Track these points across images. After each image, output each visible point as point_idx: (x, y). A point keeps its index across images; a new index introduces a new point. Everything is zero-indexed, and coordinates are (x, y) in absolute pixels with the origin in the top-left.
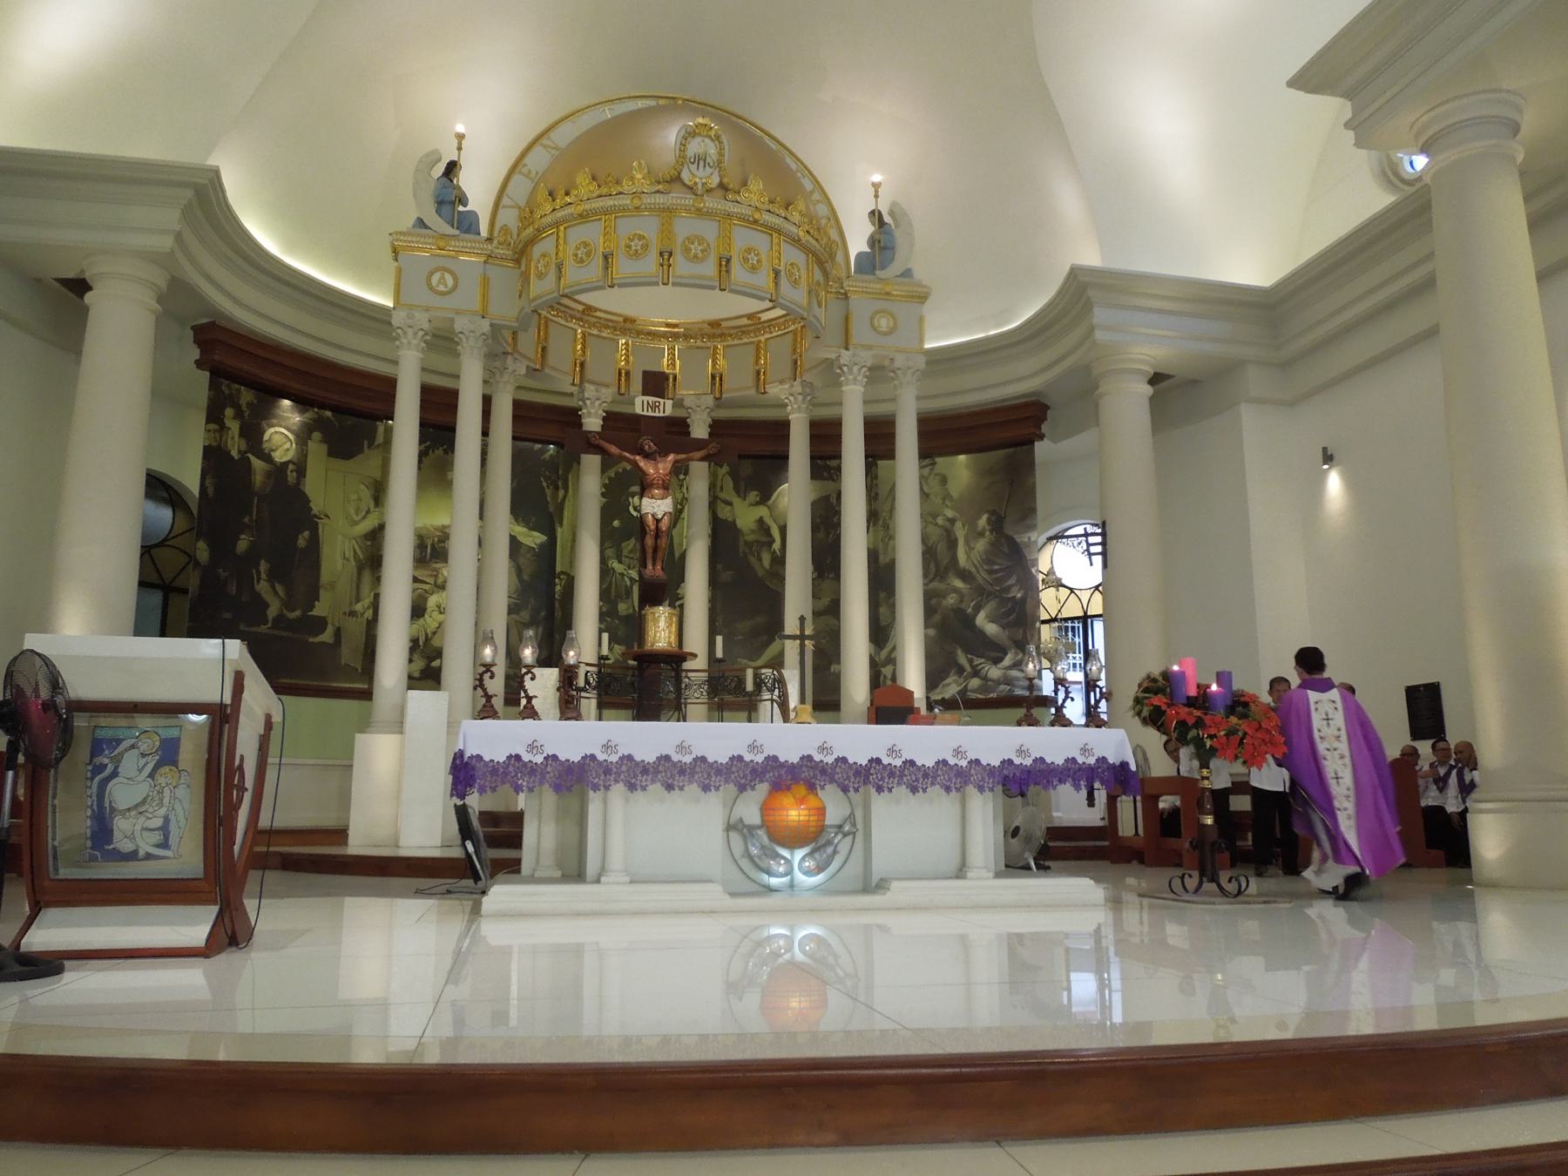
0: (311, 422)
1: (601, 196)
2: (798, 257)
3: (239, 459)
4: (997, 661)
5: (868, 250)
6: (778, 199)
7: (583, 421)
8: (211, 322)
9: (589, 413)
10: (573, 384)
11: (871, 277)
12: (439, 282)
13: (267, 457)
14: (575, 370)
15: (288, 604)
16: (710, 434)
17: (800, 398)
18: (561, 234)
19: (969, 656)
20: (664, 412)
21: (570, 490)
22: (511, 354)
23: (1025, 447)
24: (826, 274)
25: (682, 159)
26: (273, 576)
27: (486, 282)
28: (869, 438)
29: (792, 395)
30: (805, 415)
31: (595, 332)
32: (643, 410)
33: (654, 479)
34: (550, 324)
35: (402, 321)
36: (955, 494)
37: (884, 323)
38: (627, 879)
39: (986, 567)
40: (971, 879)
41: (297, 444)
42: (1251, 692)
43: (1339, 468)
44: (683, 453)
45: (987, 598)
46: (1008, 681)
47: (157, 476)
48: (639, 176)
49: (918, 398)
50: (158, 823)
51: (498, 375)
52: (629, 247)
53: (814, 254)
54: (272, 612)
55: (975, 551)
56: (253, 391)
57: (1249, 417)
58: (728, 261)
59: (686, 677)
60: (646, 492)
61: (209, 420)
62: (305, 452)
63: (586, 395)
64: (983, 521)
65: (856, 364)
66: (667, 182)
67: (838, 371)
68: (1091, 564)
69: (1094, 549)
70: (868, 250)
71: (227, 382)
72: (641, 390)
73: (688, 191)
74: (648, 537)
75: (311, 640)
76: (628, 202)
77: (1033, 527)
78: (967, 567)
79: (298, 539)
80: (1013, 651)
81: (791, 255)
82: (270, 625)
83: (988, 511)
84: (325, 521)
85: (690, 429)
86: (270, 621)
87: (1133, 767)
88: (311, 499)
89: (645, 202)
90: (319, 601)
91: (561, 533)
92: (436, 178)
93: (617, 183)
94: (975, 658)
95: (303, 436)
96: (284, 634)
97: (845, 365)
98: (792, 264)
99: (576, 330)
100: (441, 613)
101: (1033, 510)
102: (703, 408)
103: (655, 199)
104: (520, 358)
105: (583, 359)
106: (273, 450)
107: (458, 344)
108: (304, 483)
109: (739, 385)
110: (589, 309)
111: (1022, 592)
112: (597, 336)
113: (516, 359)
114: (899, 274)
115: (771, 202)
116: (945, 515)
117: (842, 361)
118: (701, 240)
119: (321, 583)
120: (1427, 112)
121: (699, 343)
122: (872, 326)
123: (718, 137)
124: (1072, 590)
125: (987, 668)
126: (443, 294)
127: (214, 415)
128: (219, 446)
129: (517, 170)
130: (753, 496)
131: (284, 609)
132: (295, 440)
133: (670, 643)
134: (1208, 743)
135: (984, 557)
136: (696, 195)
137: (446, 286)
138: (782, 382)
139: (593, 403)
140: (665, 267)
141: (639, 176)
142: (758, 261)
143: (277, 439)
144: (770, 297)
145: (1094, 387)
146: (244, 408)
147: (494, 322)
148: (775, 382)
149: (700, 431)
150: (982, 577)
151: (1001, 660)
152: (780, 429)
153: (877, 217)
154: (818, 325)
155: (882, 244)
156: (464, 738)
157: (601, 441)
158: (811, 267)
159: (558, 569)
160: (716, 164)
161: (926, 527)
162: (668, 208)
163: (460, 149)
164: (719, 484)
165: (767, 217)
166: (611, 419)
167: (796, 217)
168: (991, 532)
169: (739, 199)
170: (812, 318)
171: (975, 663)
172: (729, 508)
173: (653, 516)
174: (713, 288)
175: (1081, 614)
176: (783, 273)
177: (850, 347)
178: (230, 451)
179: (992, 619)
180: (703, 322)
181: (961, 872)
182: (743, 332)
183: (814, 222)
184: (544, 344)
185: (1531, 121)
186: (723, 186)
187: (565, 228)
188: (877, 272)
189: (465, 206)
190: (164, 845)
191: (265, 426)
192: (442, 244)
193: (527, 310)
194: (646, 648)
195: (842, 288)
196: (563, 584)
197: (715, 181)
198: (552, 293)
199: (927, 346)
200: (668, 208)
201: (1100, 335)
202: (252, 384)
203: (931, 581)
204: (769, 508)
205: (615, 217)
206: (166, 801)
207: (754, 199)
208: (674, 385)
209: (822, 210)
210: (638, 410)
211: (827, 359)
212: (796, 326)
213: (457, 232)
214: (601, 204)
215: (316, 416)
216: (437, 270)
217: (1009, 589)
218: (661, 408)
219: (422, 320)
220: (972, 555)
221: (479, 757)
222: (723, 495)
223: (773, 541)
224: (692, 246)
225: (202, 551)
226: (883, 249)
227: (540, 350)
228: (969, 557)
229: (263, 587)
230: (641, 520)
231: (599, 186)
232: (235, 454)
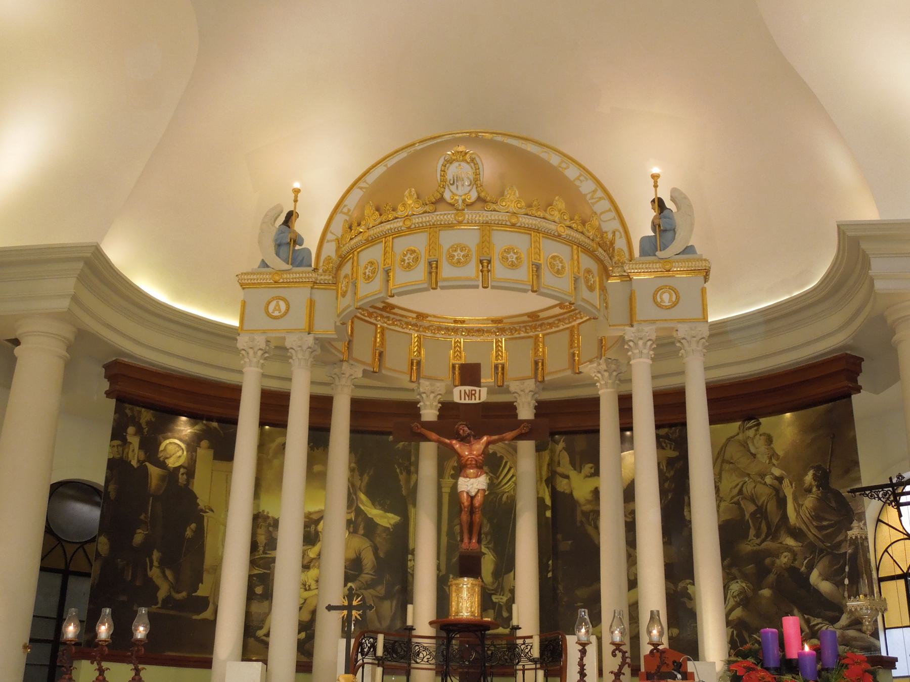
0: (201, 433)
1: (382, 223)
2: (562, 251)
3: (138, 467)
5: (654, 234)
6: (535, 203)
7: (421, 412)
8: (115, 360)
9: (425, 405)
10: (411, 381)
11: (653, 258)
12: (275, 309)
13: (162, 465)
14: (412, 369)
15: (176, 587)
16: (536, 415)
17: (606, 374)
19: (806, 616)
20: (480, 399)
22: (345, 361)
23: (844, 400)
25: (444, 184)
26: (163, 564)
27: (312, 304)
29: (599, 372)
31: (429, 334)
32: (461, 399)
33: (467, 460)
34: (387, 333)
35: (245, 344)
36: (781, 453)
37: (666, 298)
41: (187, 452)
44: (495, 435)
45: (819, 554)
47: (91, 485)
48: (410, 202)
51: (337, 379)
52: (403, 261)
53: (579, 245)
54: (162, 594)
55: (804, 507)
56: (152, 411)
58: (489, 262)
59: (493, 644)
60: (463, 471)
61: (114, 437)
62: (194, 457)
63: (422, 390)
64: (809, 478)
65: (641, 339)
66: (432, 203)
71: (131, 406)
73: (450, 208)
74: (463, 513)
75: (195, 617)
76: (401, 224)
79: (186, 531)
81: (550, 249)
82: (159, 605)
83: (813, 467)
84: (210, 513)
85: (518, 411)
86: (160, 602)
88: (198, 496)
89: (414, 221)
90: (202, 584)
91: (412, 511)
92: (277, 227)
93: (393, 210)
94: (812, 618)
95: (193, 445)
96: (172, 612)
97: (631, 340)
98: (554, 258)
100: (306, 590)
101: (856, 463)
102: (527, 391)
104: (353, 363)
105: (418, 359)
106: (167, 458)
107: (291, 357)
108: (193, 483)
110: (421, 316)
113: (352, 365)
115: (529, 206)
116: (772, 474)
119: (205, 567)
121: (523, 334)
123: (473, 160)
125: (824, 628)
126: (276, 318)
127: (118, 434)
128: (121, 458)
129: (339, 210)
130: (588, 468)
131: (171, 590)
132: (187, 448)
133: (472, 613)
136: (457, 210)
137: (280, 311)
138: (591, 361)
140: (433, 274)
141: (410, 202)
142: (516, 258)
143: (171, 448)
144: (530, 288)
146: (144, 425)
147: (317, 336)
148: (586, 362)
149: (526, 413)
150: (812, 534)
152: (592, 405)
153: (659, 204)
155: (662, 228)
157: (422, 429)
158: (575, 257)
159: (411, 547)
160: (473, 182)
161: (755, 487)
162: (434, 225)
163: (296, 201)
164: (556, 459)
167: (557, 216)
168: (818, 487)
170: (583, 304)
171: (812, 624)
172: (565, 481)
173: (467, 493)
174: (477, 287)
177: (635, 324)
178: (130, 461)
179: (826, 578)
182: (559, 320)
183: (576, 217)
184: (382, 350)
186: (480, 199)
189: (301, 245)
191: (161, 438)
192: (277, 278)
193: (338, 324)
194: (450, 617)
195: (625, 272)
197: (474, 196)
198: (349, 306)
200: (434, 225)
201: (879, 285)
202: (149, 406)
203: (764, 541)
205: (393, 239)
207: (512, 207)
208: (503, 374)
210: (456, 399)
211: (620, 336)
213: (289, 267)
214: (381, 228)
215: (205, 427)
216: (273, 299)
218: (477, 395)
219: (260, 341)
222: (560, 470)
224: (455, 254)
225: (103, 546)
226: (665, 231)
227: (377, 355)
228: (798, 513)
229: (154, 573)
231: (381, 215)
232: (134, 463)
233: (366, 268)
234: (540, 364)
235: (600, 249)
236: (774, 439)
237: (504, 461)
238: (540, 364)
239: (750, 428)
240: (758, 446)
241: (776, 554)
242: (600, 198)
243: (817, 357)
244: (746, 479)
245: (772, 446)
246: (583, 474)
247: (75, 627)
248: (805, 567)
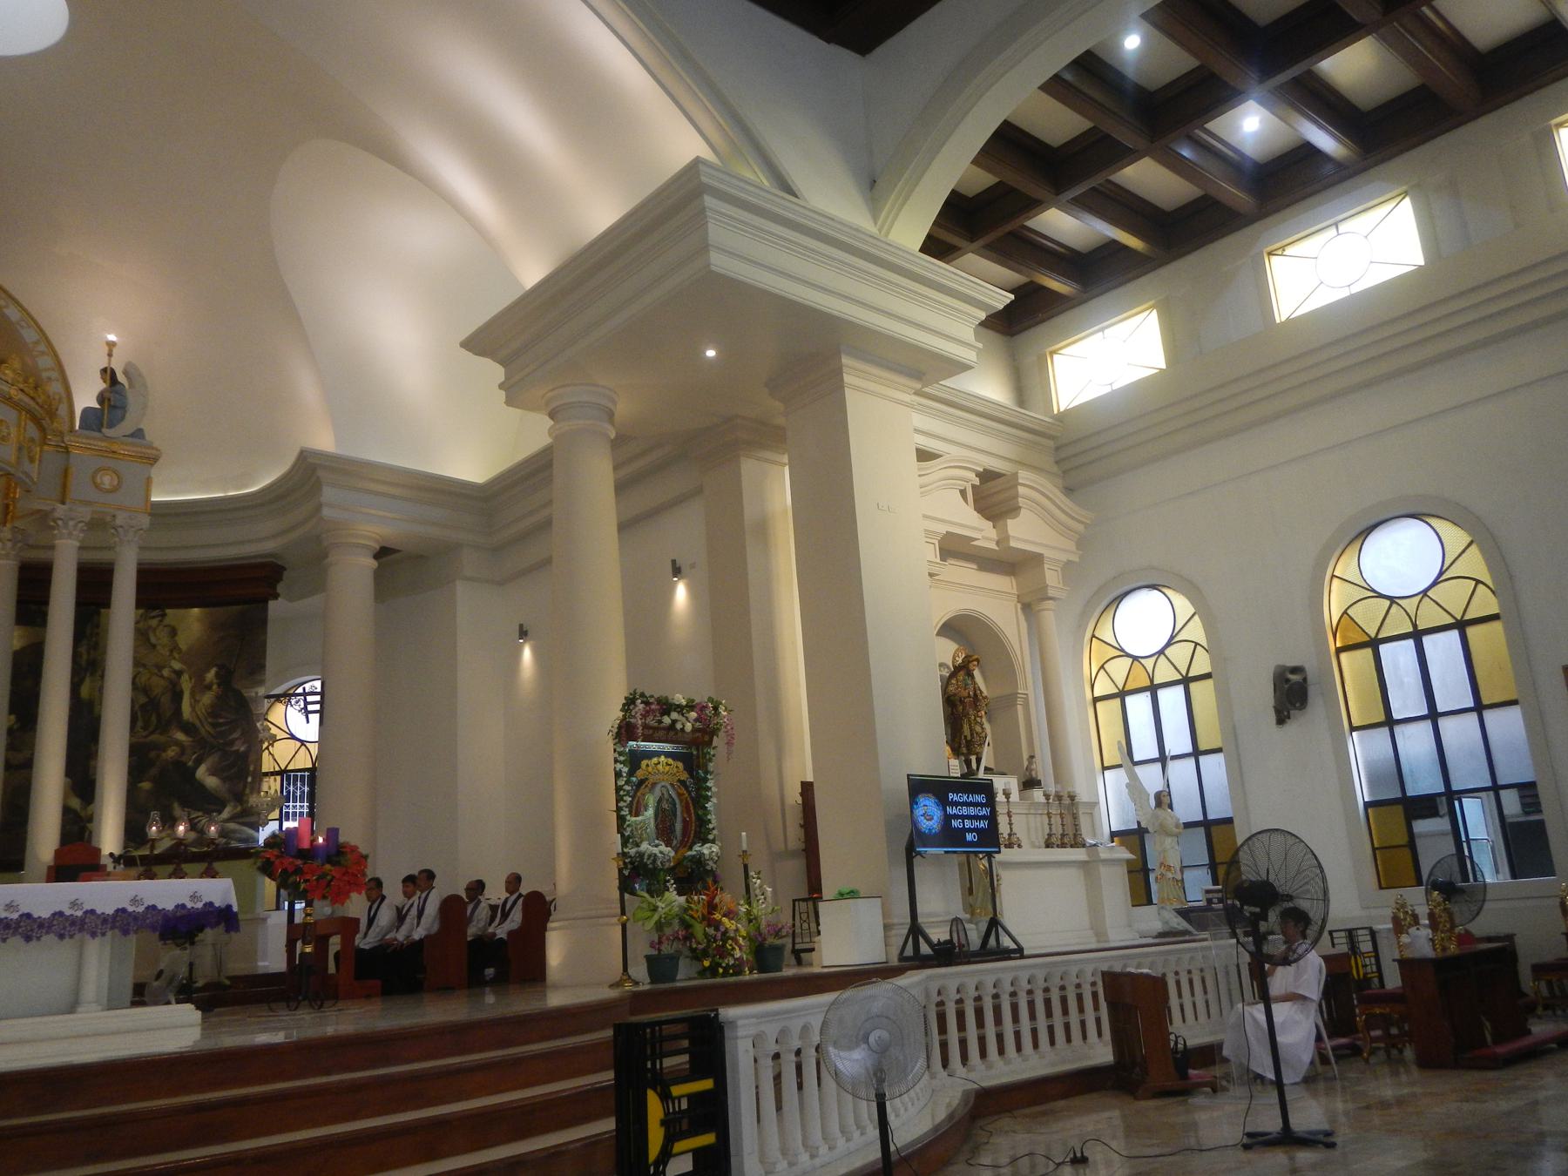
5: (98, 406)
17: (9, 544)
24: (42, 429)
30: (15, 563)
36: (183, 647)
37: (107, 480)
39: (210, 720)
40: (81, 1013)
42: (353, 844)
43: (532, 642)
53: (29, 411)
57: (462, 590)
64: (211, 675)
65: (72, 519)
67: (52, 524)
68: (308, 722)
69: (310, 708)
70: (98, 406)
77: (261, 683)
78: (191, 720)
83: (216, 665)
87: (235, 909)
94: (193, 812)
101: (262, 667)
111: (246, 746)
114: (127, 434)
116: (171, 667)
117: (56, 515)
122: (97, 486)
124: (303, 743)
134: (302, 886)
145: (326, 556)
150: (205, 729)
151: (220, 812)
153: (109, 375)
154: (27, 480)
158: (23, 423)
161: (149, 679)
168: (219, 685)
170: (21, 475)
175: (311, 766)
177: (68, 501)
179: (213, 772)
181: (72, 1007)
183: (31, 380)
185: (624, 408)
188: (104, 430)
195: (63, 442)
201: (326, 512)
203: (152, 733)
209: (44, 362)
211: (39, 511)
217: (232, 743)
220: (197, 709)
228: (193, 707)
235: (47, 419)
236: (179, 633)
239: (154, 617)
240: (161, 638)
241: (163, 748)
242: (43, 353)
245: (177, 638)
248: (194, 762)
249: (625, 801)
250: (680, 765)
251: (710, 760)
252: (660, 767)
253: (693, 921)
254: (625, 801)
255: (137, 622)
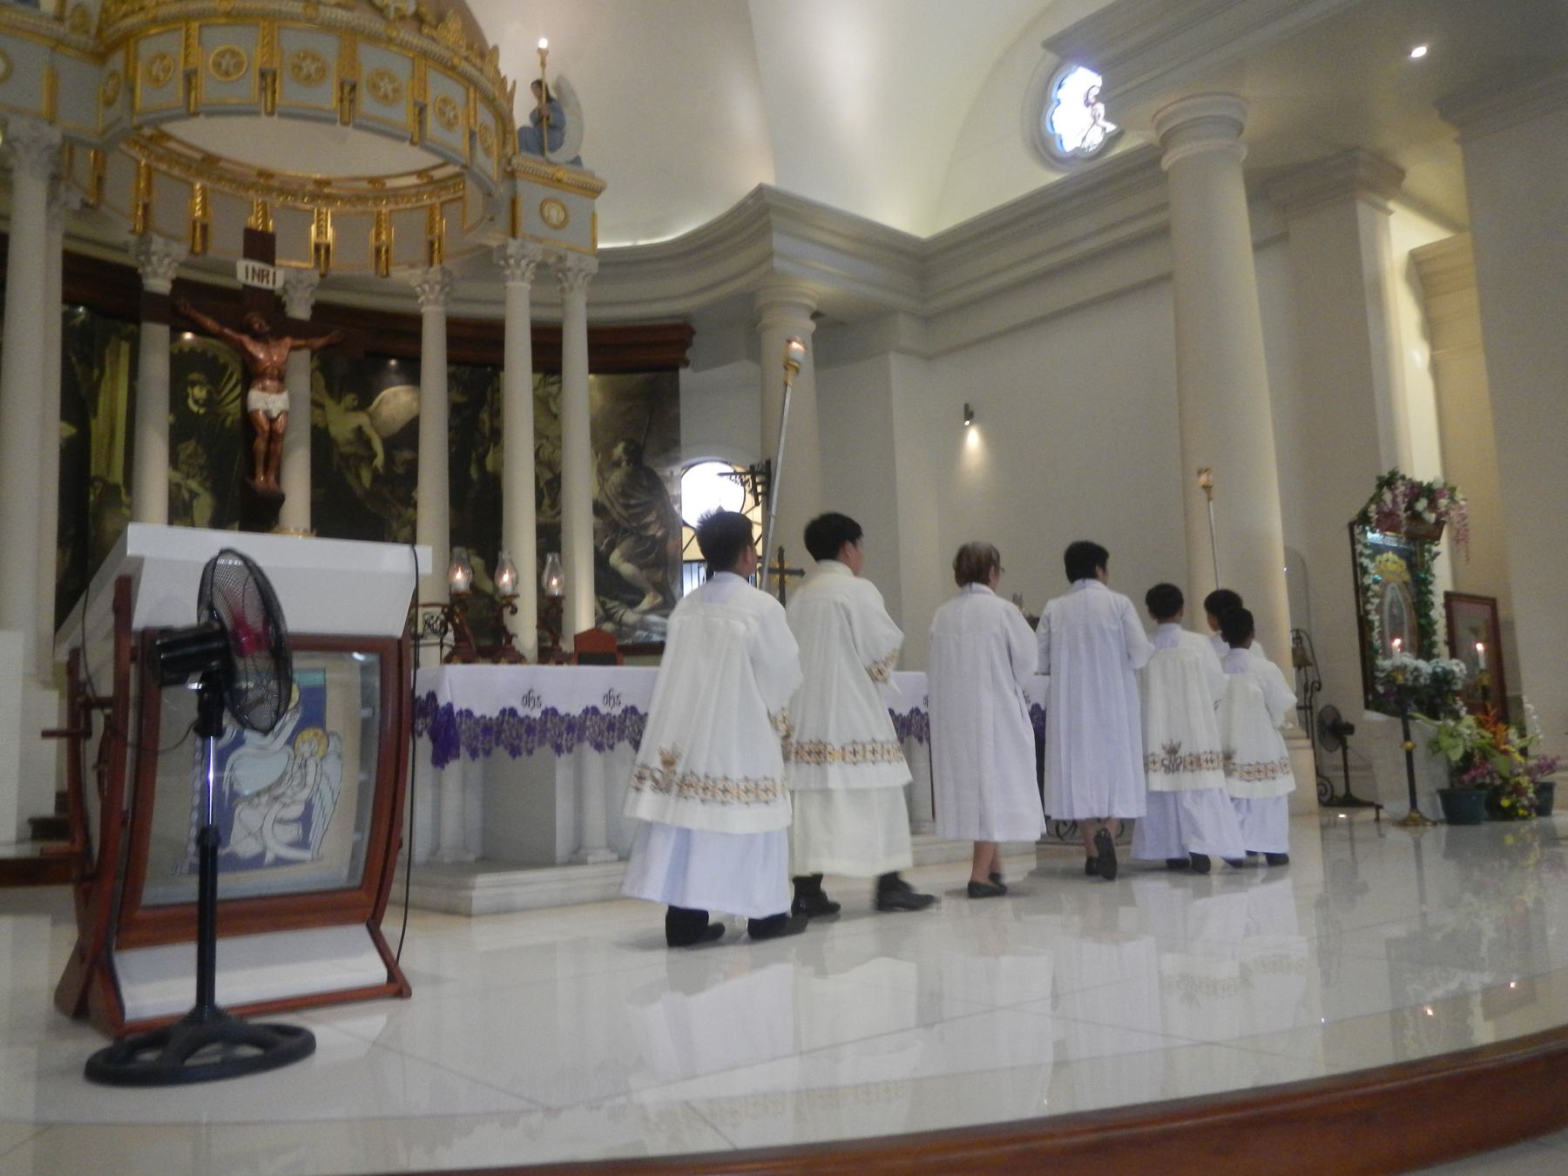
4: (633, 604)
10: (133, 232)
11: (540, 158)
16: (312, 317)
17: (437, 288)
18: (194, 32)
21: (108, 370)
27: (54, 75)
28: (536, 346)
29: (426, 282)
31: (163, 167)
32: (247, 277)
33: (268, 367)
37: (554, 214)
38: (615, 857)
39: (621, 501)
45: (623, 534)
46: (645, 626)
49: (588, 305)
50: (297, 810)
52: (300, 68)
55: (610, 482)
57: (896, 364)
58: (422, 110)
63: (153, 248)
64: (619, 450)
65: (524, 257)
67: (502, 263)
72: (241, 248)
80: (651, 594)
91: (93, 423)
94: (608, 601)
97: (511, 257)
99: (138, 162)
101: (676, 443)
103: (331, 14)
109: (353, 263)
112: (165, 174)
118: (392, 80)
120: (1181, 100)
125: (621, 612)
130: (350, 399)
135: (620, 490)
138: (412, 266)
139: (160, 261)
149: (300, 310)
151: (637, 603)
156: (450, 684)
159: (93, 473)
161: (553, 452)
165: (465, 66)
166: (178, 283)
168: (629, 462)
169: (435, 35)
176: (478, 136)
177: (519, 234)
179: (628, 558)
180: (309, 179)
186: (419, 18)
187: (200, 27)
188: (548, 154)
190: (303, 843)
196: (98, 491)
197: (410, 8)
199: (601, 245)
201: (777, 263)
204: (371, 416)
206: (310, 779)
211: (481, 246)
212: (436, 201)
217: (646, 527)
221: (469, 713)
223: (374, 456)
224: (382, 84)
226: (552, 127)
230: (248, 418)
233: (222, 54)
234: (323, 251)
237: (228, 372)
238: (323, 251)
243: (641, 320)
244: (544, 441)
246: (343, 405)
247: (465, 574)
249: (1372, 604)
250: (1403, 563)
251: (1433, 558)
252: (1389, 564)
253: (1494, 752)
254: (1372, 604)
255: (535, 389)
